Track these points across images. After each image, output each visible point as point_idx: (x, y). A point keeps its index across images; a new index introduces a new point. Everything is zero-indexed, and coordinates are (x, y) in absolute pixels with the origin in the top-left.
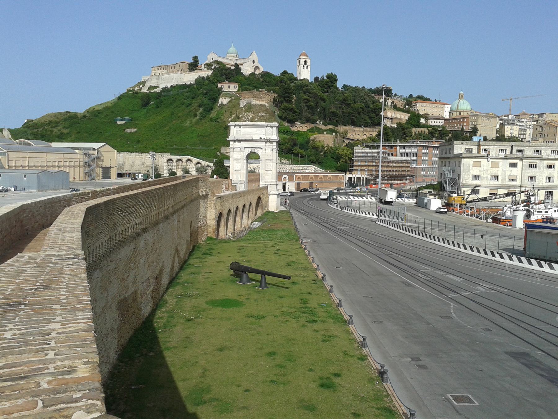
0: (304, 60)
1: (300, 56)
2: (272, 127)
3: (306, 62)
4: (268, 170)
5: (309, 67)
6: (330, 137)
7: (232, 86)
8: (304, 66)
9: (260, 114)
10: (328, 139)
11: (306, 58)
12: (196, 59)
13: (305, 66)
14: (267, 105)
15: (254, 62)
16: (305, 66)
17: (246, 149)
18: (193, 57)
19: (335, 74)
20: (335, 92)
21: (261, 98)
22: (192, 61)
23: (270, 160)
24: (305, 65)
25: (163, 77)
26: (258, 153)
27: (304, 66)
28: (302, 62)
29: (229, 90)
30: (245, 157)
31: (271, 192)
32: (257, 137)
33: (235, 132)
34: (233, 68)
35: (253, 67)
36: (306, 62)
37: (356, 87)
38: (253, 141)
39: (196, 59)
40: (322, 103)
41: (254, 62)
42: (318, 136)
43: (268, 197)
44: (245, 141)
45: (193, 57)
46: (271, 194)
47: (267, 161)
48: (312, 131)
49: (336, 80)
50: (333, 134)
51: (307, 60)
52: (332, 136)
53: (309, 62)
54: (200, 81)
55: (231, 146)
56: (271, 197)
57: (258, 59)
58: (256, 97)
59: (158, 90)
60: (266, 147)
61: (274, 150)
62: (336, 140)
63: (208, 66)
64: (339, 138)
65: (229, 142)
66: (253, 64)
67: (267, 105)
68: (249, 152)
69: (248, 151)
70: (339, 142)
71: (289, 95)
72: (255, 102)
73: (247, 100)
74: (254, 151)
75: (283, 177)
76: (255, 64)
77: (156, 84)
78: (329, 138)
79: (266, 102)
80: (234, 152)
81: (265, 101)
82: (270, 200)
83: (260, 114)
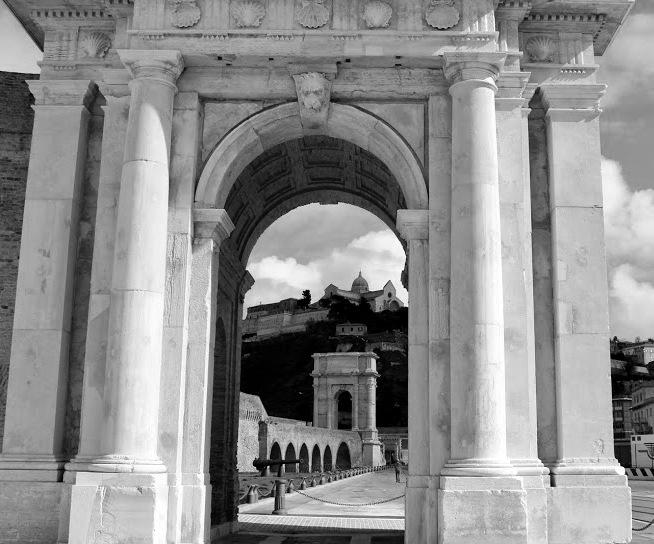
7: (355, 328)
9: (392, 364)
12: (307, 293)
25: (263, 320)
29: (352, 333)
32: (345, 371)
34: (357, 304)
38: (341, 375)
39: (307, 293)
44: (333, 375)
54: (311, 325)
58: (387, 341)
59: (253, 339)
63: (324, 302)
65: (312, 379)
66: (387, 299)
69: (336, 389)
72: (385, 347)
73: (374, 345)
77: (251, 331)
83: (392, 364)
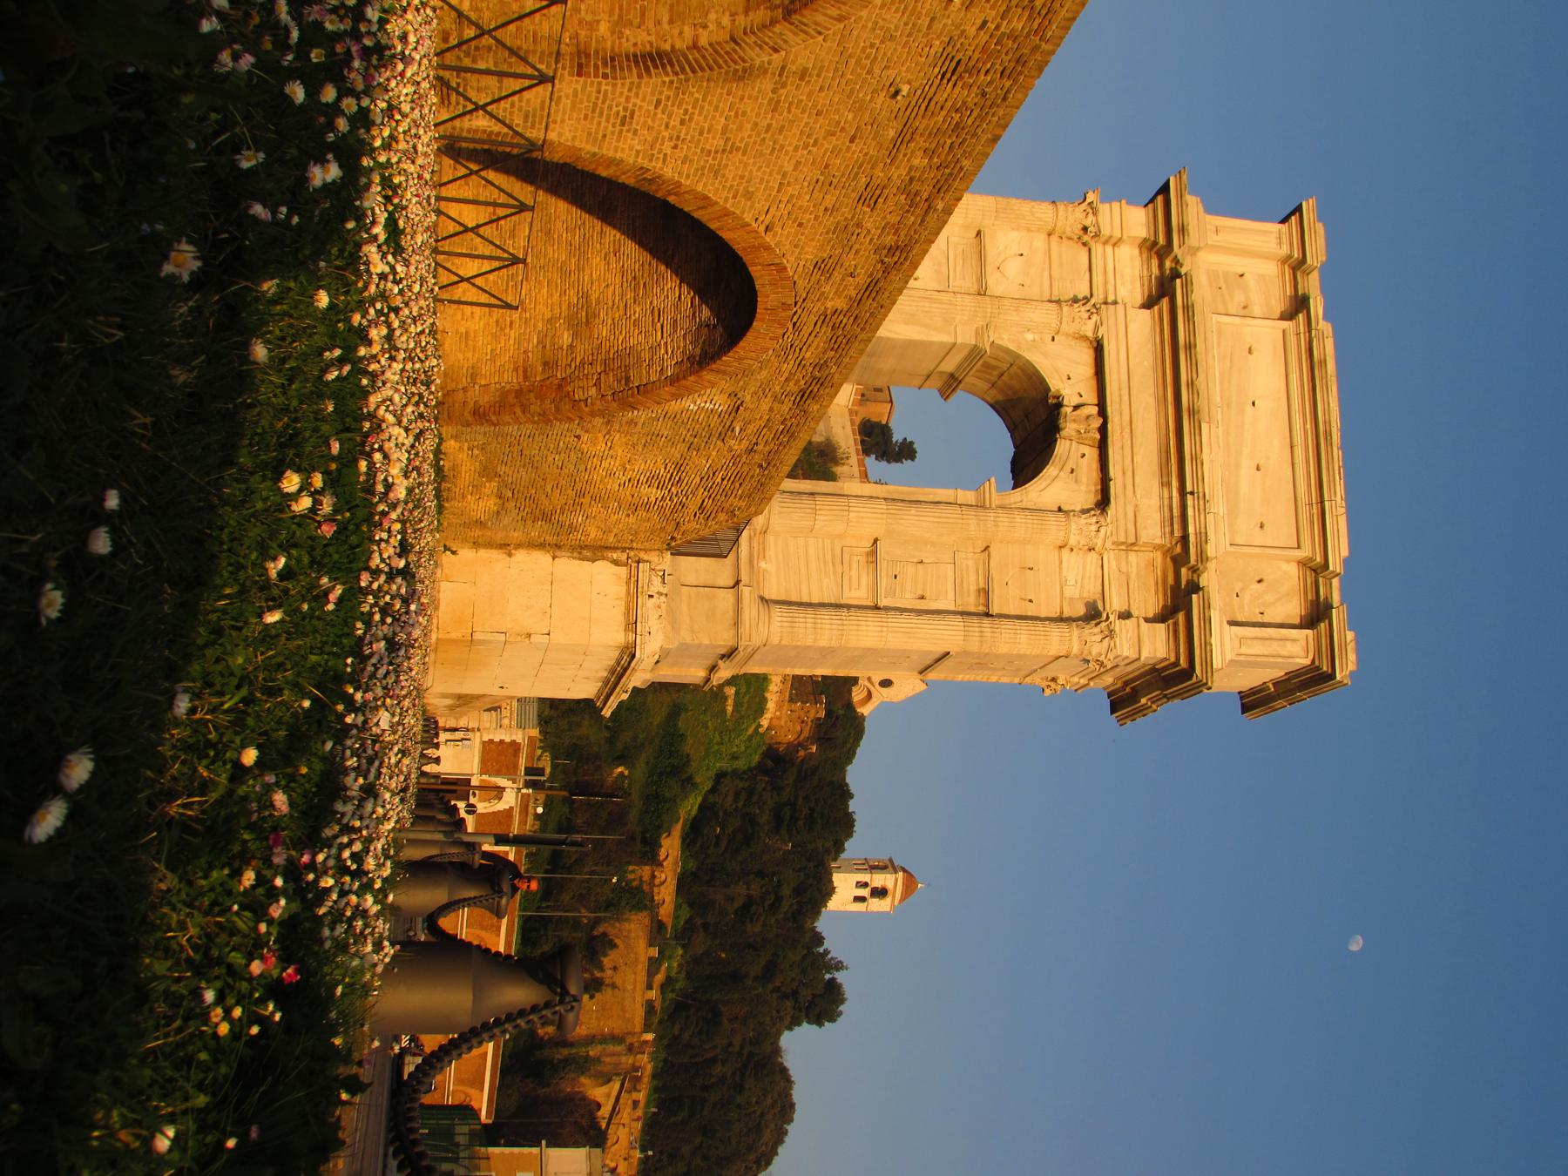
0: (890, 885)
1: (904, 870)
2: (1316, 615)
3: (880, 893)
4: (882, 565)
5: (860, 907)
6: (630, 1020)
8: (866, 885)
10: (623, 1011)
11: (898, 896)
13: (865, 892)
14: (765, 723)
15: (886, 683)
16: (865, 892)
17: (1087, 356)
18: (912, 443)
19: (841, 1013)
20: (781, 1019)
21: (791, 700)
22: (897, 437)
23: (987, 593)
24: (869, 889)
26: (1050, 471)
27: (866, 885)
28: (879, 880)
30: (1006, 339)
31: (657, 585)
33: (1237, 264)
35: (869, 679)
36: (880, 893)
37: (792, 1106)
40: (756, 970)
41: (886, 683)
42: (637, 960)
43: (593, 551)
45: (912, 443)
46: (633, 583)
47: (969, 562)
48: (658, 928)
49: (819, 1023)
50: (646, 1031)
51: (888, 901)
52: (638, 1028)
53: (877, 905)
55: (1104, 209)
56: (605, 577)
57: (895, 700)
60: (1110, 559)
61: (1093, 633)
62: (618, 1048)
64: (624, 1059)
66: (877, 679)
67: (765, 723)
68: (1055, 384)
70: (608, 1060)
71: (801, 823)
74: (1063, 433)
75: (501, 781)
76: (877, 686)
78: (627, 1015)
79: (775, 722)
80: (1039, 242)
81: (779, 718)
82: (569, 567)
